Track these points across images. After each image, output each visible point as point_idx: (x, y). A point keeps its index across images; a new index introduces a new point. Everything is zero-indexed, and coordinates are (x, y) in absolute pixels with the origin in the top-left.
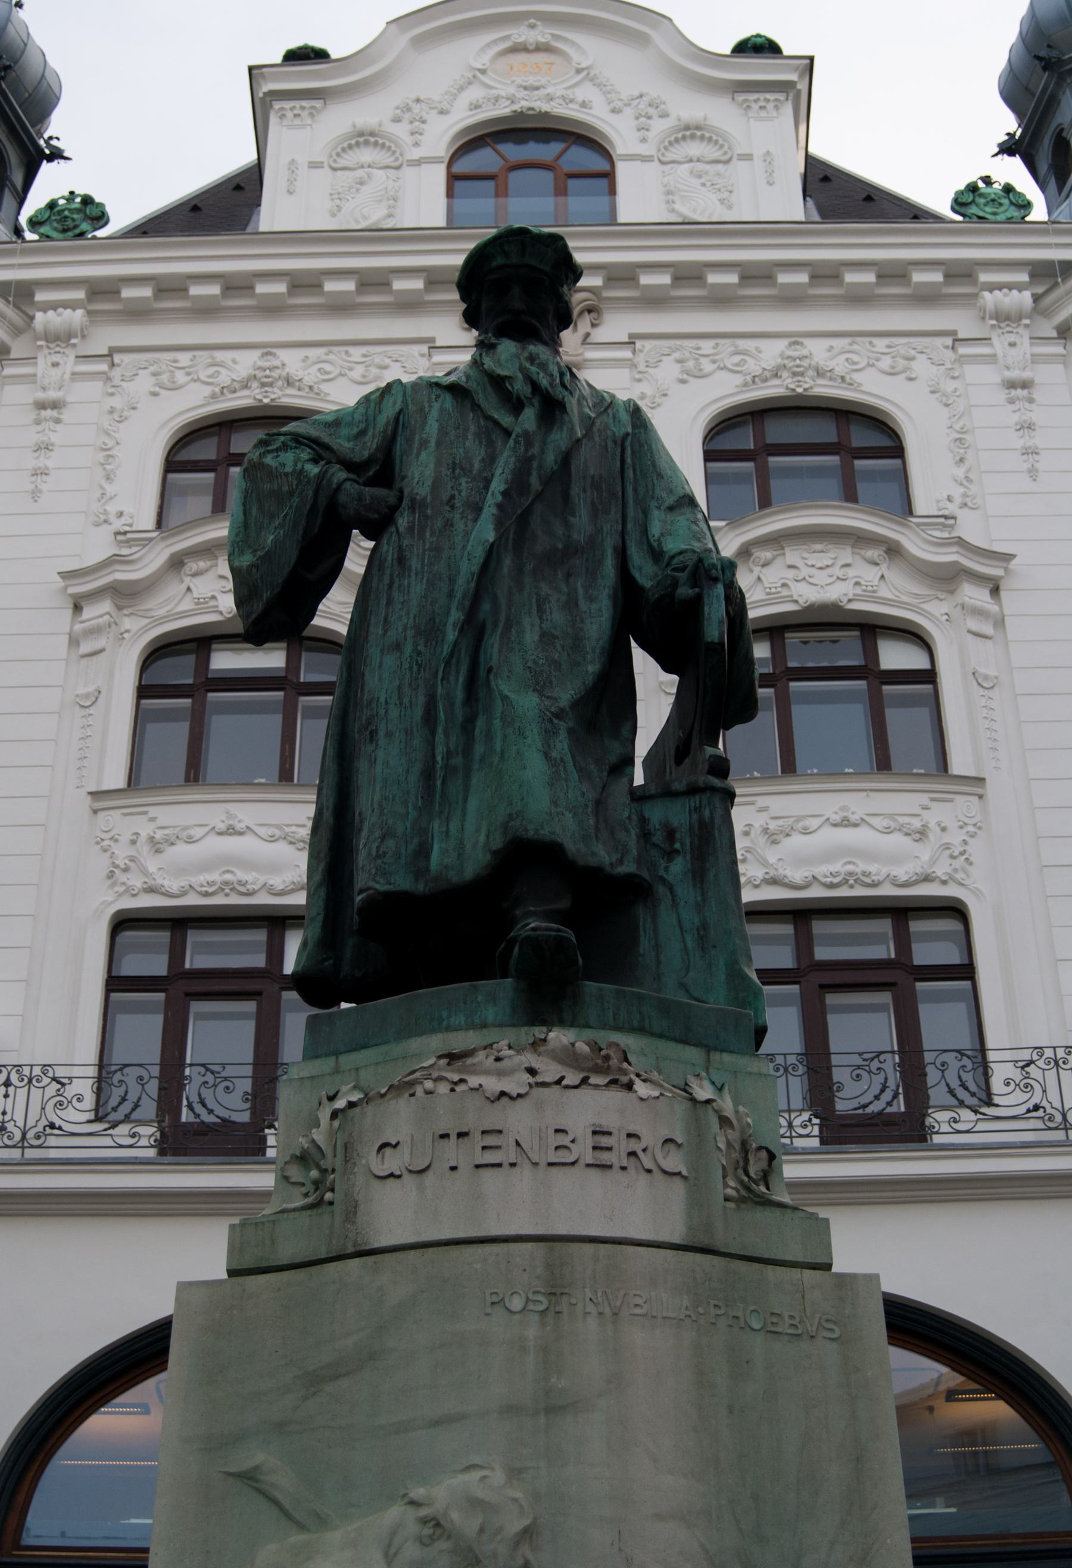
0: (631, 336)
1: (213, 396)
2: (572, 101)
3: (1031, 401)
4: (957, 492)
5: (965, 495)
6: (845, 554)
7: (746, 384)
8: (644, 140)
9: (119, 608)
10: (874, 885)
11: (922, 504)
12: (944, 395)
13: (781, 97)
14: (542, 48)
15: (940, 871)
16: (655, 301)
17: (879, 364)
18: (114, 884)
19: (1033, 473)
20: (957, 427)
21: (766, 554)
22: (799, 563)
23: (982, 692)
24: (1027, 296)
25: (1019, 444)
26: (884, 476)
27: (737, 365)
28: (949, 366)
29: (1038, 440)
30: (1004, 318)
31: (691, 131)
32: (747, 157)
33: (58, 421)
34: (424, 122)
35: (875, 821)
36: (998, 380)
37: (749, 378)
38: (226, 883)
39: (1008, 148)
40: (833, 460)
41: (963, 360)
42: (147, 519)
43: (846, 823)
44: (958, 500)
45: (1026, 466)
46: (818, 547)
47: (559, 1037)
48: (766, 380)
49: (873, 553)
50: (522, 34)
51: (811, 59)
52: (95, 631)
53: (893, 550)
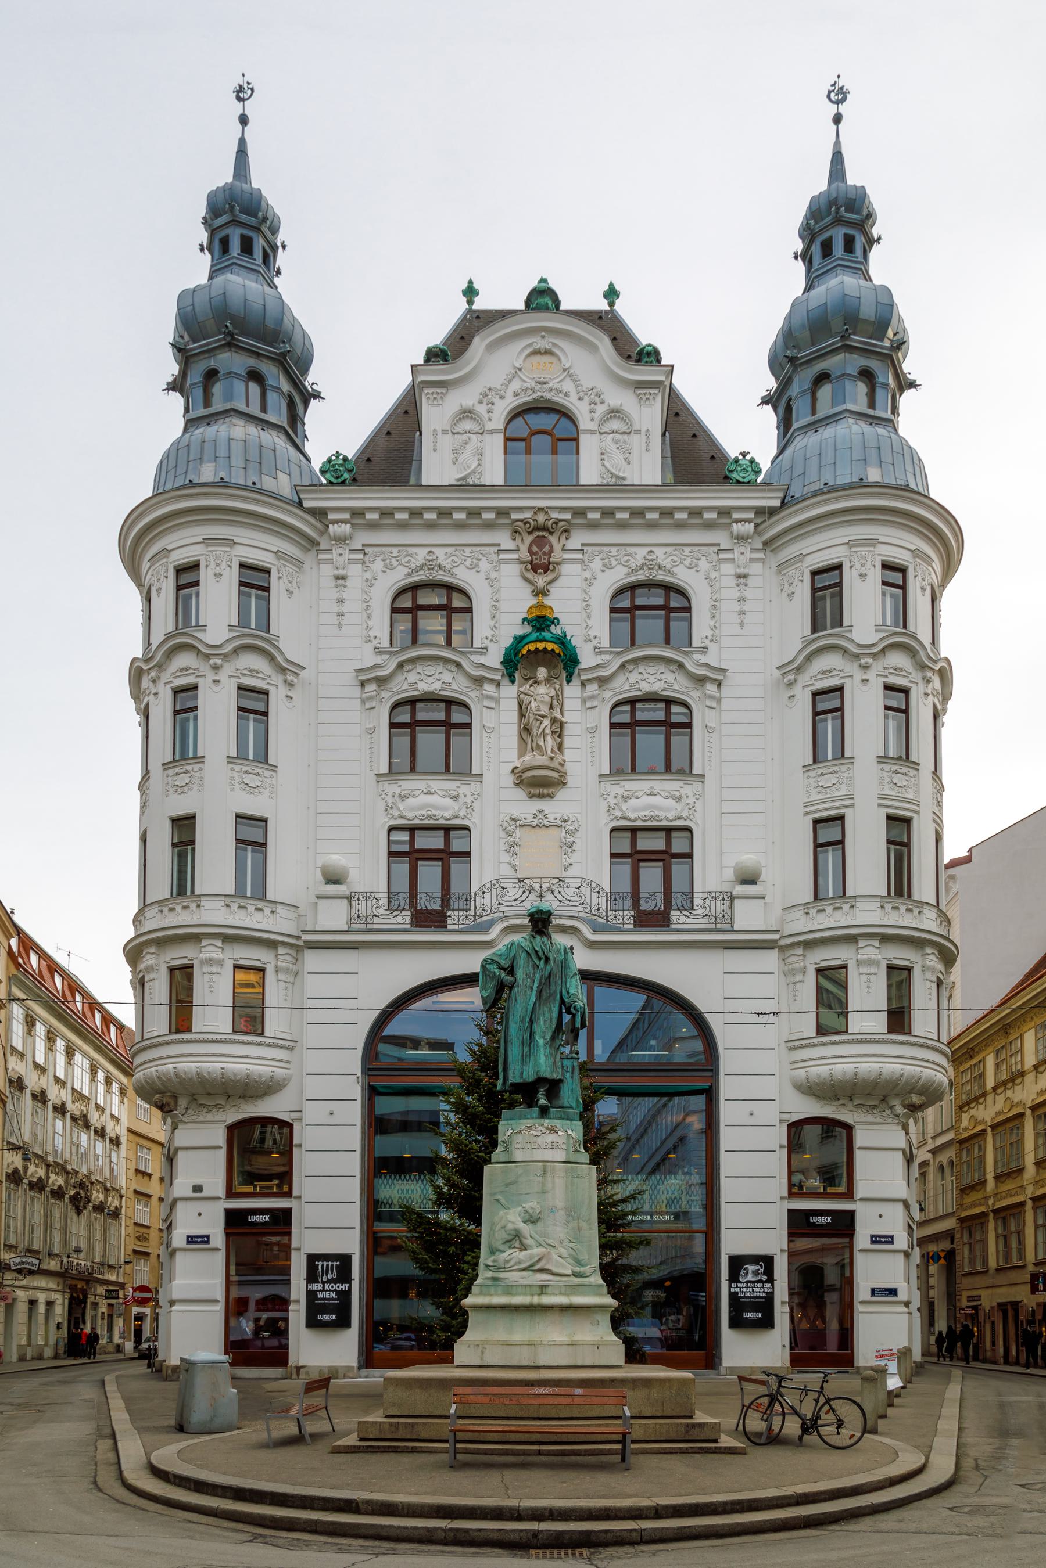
0: (583, 545)
1: (409, 575)
2: (561, 391)
3: (746, 585)
4: (709, 633)
5: (713, 636)
6: (662, 668)
7: (629, 574)
8: (592, 420)
9: (379, 686)
10: (660, 821)
11: (696, 642)
12: (711, 580)
13: (656, 391)
14: (548, 352)
15: (685, 814)
16: (594, 526)
17: (685, 562)
18: (387, 814)
19: (742, 624)
20: (714, 598)
21: (630, 667)
22: (643, 671)
23: (708, 734)
24: (751, 527)
25: (738, 608)
26: (682, 619)
27: (626, 562)
28: (714, 564)
29: (747, 607)
30: (741, 538)
31: (615, 413)
32: (638, 432)
33: (345, 586)
34: (493, 404)
35: (662, 793)
36: (733, 573)
37: (630, 570)
38: (429, 815)
39: (765, 401)
40: (663, 612)
41: (721, 561)
42: (386, 643)
43: (652, 794)
44: (710, 638)
45: (739, 621)
46: (651, 664)
47: (546, 1122)
48: (637, 571)
49: (673, 667)
50: (539, 343)
51: (672, 366)
52: (371, 698)
53: (681, 666)
